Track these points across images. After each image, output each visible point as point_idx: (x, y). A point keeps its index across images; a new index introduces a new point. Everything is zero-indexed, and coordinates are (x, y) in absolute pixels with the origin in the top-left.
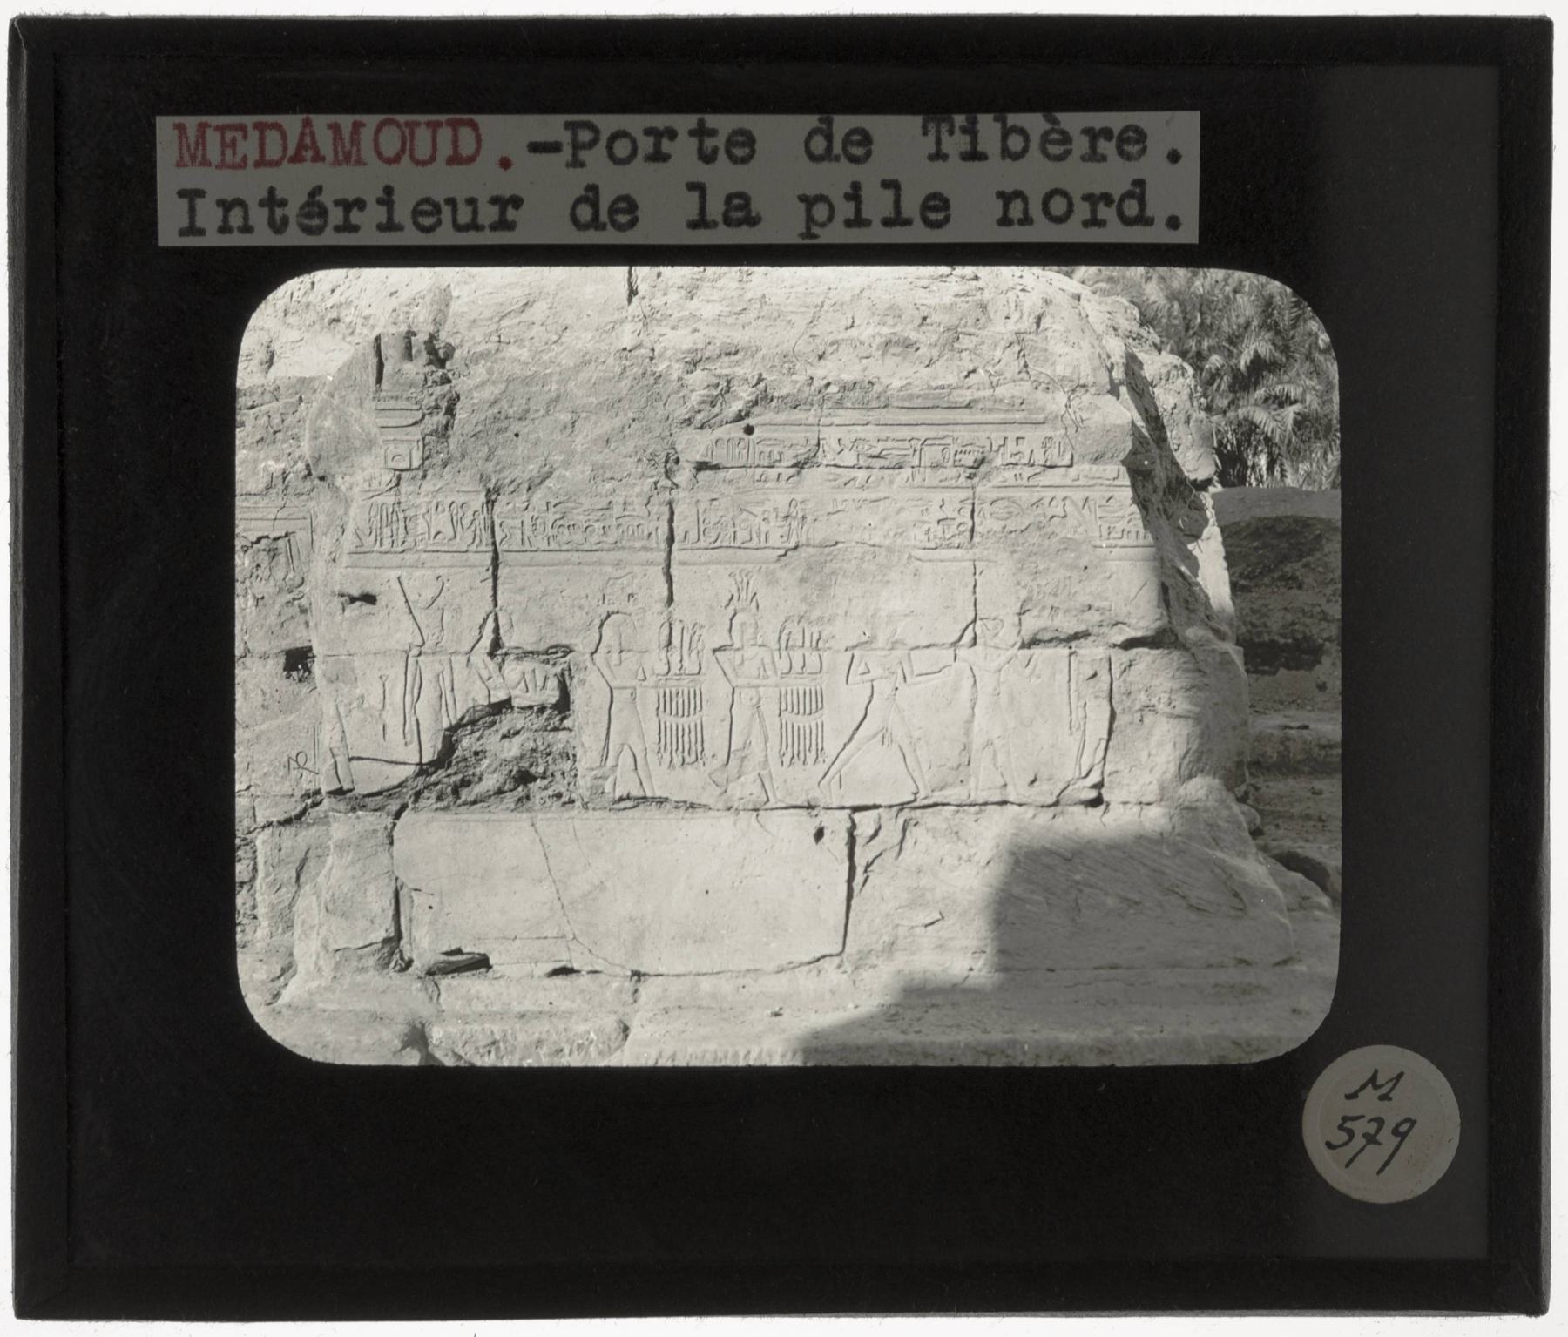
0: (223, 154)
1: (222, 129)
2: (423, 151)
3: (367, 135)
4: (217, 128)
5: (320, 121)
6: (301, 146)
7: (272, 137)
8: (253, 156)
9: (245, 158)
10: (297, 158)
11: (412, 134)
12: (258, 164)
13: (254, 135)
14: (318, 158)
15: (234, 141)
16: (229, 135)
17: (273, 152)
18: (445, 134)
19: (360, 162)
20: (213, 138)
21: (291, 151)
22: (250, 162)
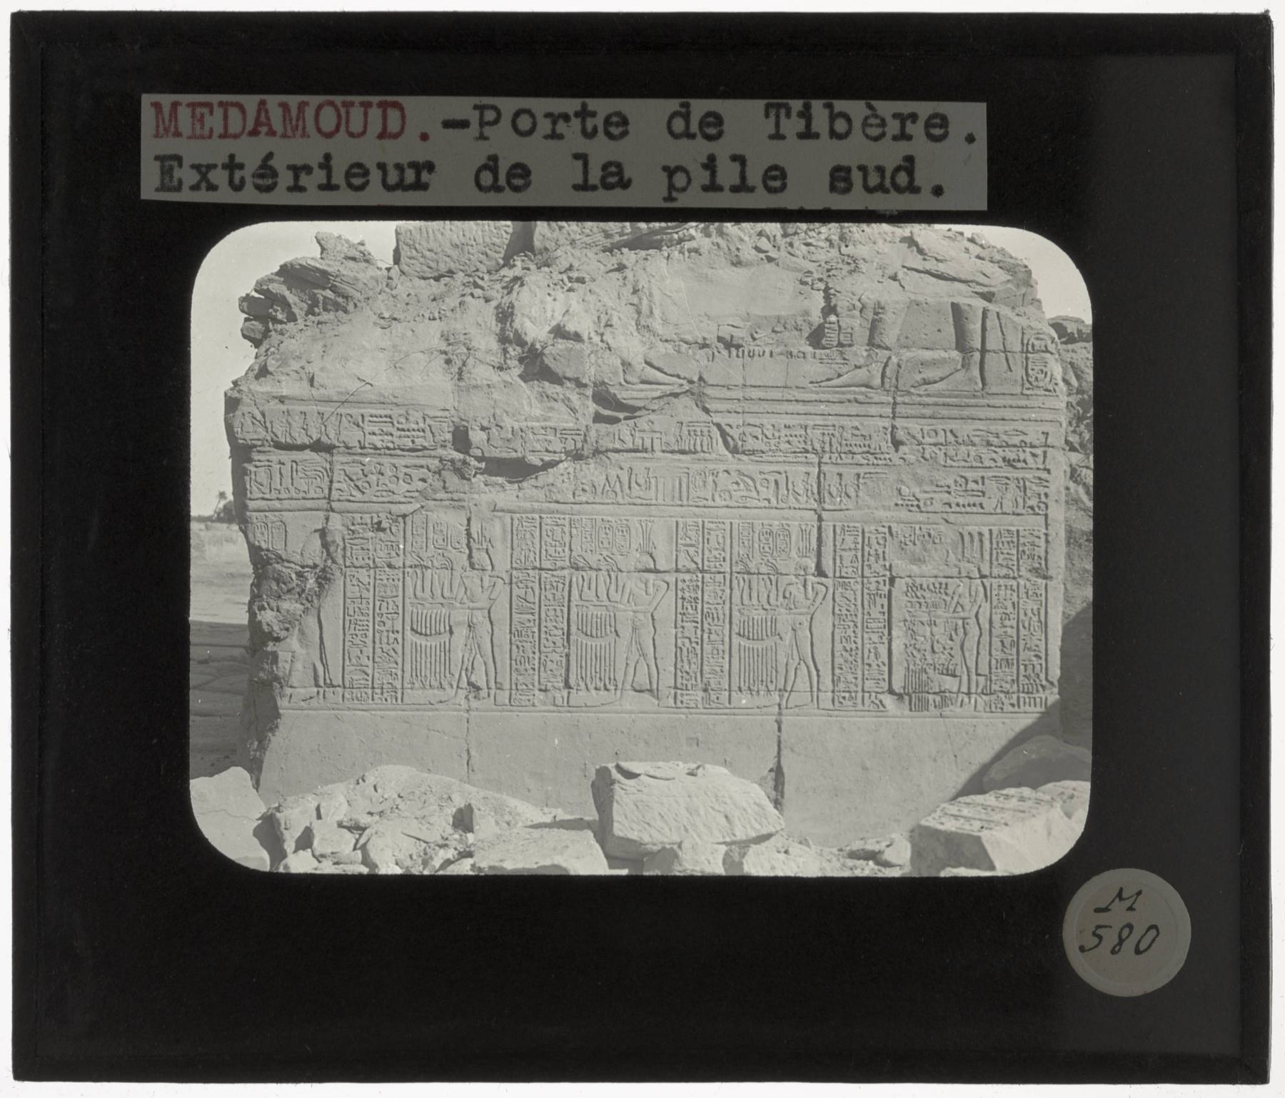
0: (193, 129)
1: (193, 105)
2: (356, 126)
3: (309, 113)
4: (188, 105)
5: (273, 101)
6: (258, 123)
7: (234, 113)
8: (219, 129)
9: (211, 130)
10: (254, 133)
11: (348, 113)
12: (221, 137)
13: (218, 112)
14: (272, 133)
15: (202, 115)
16: (199, 110)
17: (235, 127)
18: (375, 113)
19: (304, 135)
20: (184, 113)
21: (250, 125)
22: (215, 134)
